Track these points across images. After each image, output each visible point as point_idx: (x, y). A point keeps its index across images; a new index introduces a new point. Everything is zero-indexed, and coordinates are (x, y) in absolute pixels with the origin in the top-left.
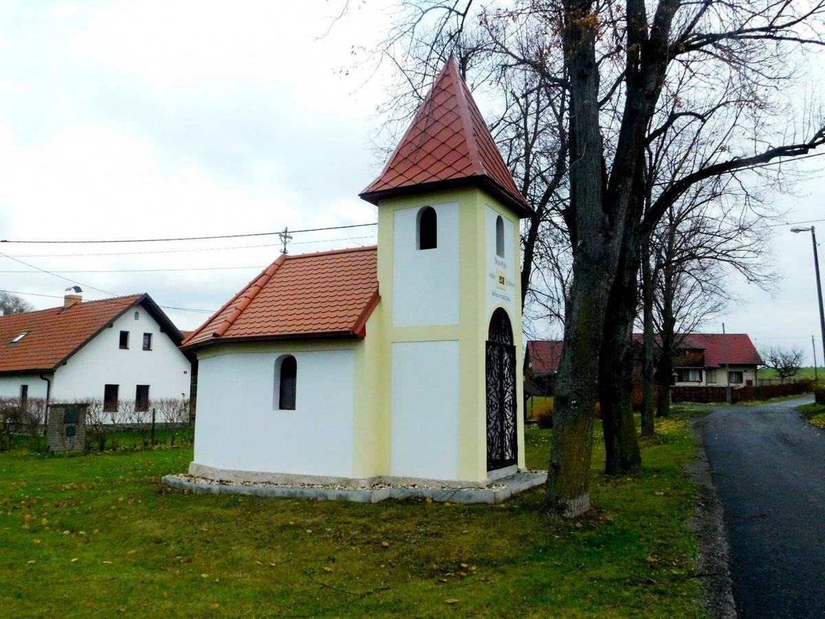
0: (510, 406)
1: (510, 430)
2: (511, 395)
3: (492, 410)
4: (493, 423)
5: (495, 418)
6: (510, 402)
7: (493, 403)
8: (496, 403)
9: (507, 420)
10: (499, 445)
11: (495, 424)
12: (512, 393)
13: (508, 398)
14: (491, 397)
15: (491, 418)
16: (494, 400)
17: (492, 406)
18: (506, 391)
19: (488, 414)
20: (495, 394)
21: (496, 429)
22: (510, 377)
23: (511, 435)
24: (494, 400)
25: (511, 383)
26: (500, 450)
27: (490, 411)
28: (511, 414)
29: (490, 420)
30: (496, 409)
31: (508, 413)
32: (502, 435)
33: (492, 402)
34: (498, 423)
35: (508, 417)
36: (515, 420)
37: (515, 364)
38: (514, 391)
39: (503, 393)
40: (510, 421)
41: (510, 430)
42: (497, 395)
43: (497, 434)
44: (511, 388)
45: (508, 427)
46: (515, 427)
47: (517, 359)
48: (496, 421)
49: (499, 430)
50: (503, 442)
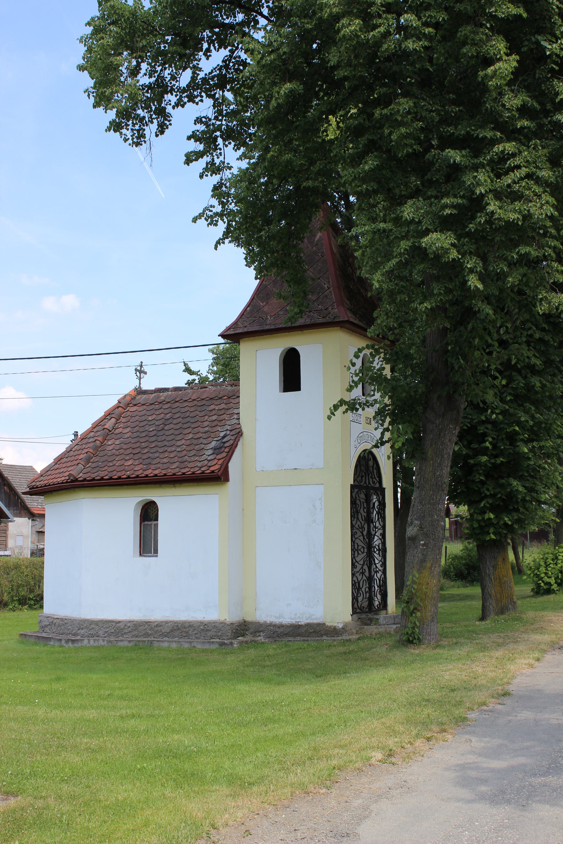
0: (379, 550)
1: (379, 575)
2: (380, 539)
3: (358, 554)
4: (359, 567)
5: (362, 562)
6: (379, 546)
7: (360, 547)
8: (364, 548)
9: (375, 564)
10: (367, 589)
11: (362, 568)
12: (381, 537)
13: (377, 541)
14: (357, 541)
15: (357, 562)
16: (360, 543)
17: (358, 550)
18: (375, 535)
19: (353, 558)
20: (361, 538)
21: (363, 573)
22: (378, 519)
23: (380, 580)
24: (360, 543)
25: (380, 527)
26: (368, 595)
27: (356, 555)
28: (380, 558)
29: (356, 564)
30: (363, 553)
31: (377, 558)
32: (370, 579)
33: (358, 546)
34: (365, 567)
35: (377, 561)
36: (384, 564)
37: (385, 507)
38: (383, 535)
39: (370, 537)
40: (378, 565)
41: (379, 575)
42: (364, 538)
43: (364, 578)
44: (381, 531)
45: (377, 572)
46: (384, 572)
47: (386, 501)
48: (363, 565)
49: (367, 574)
50: (370, 587)
